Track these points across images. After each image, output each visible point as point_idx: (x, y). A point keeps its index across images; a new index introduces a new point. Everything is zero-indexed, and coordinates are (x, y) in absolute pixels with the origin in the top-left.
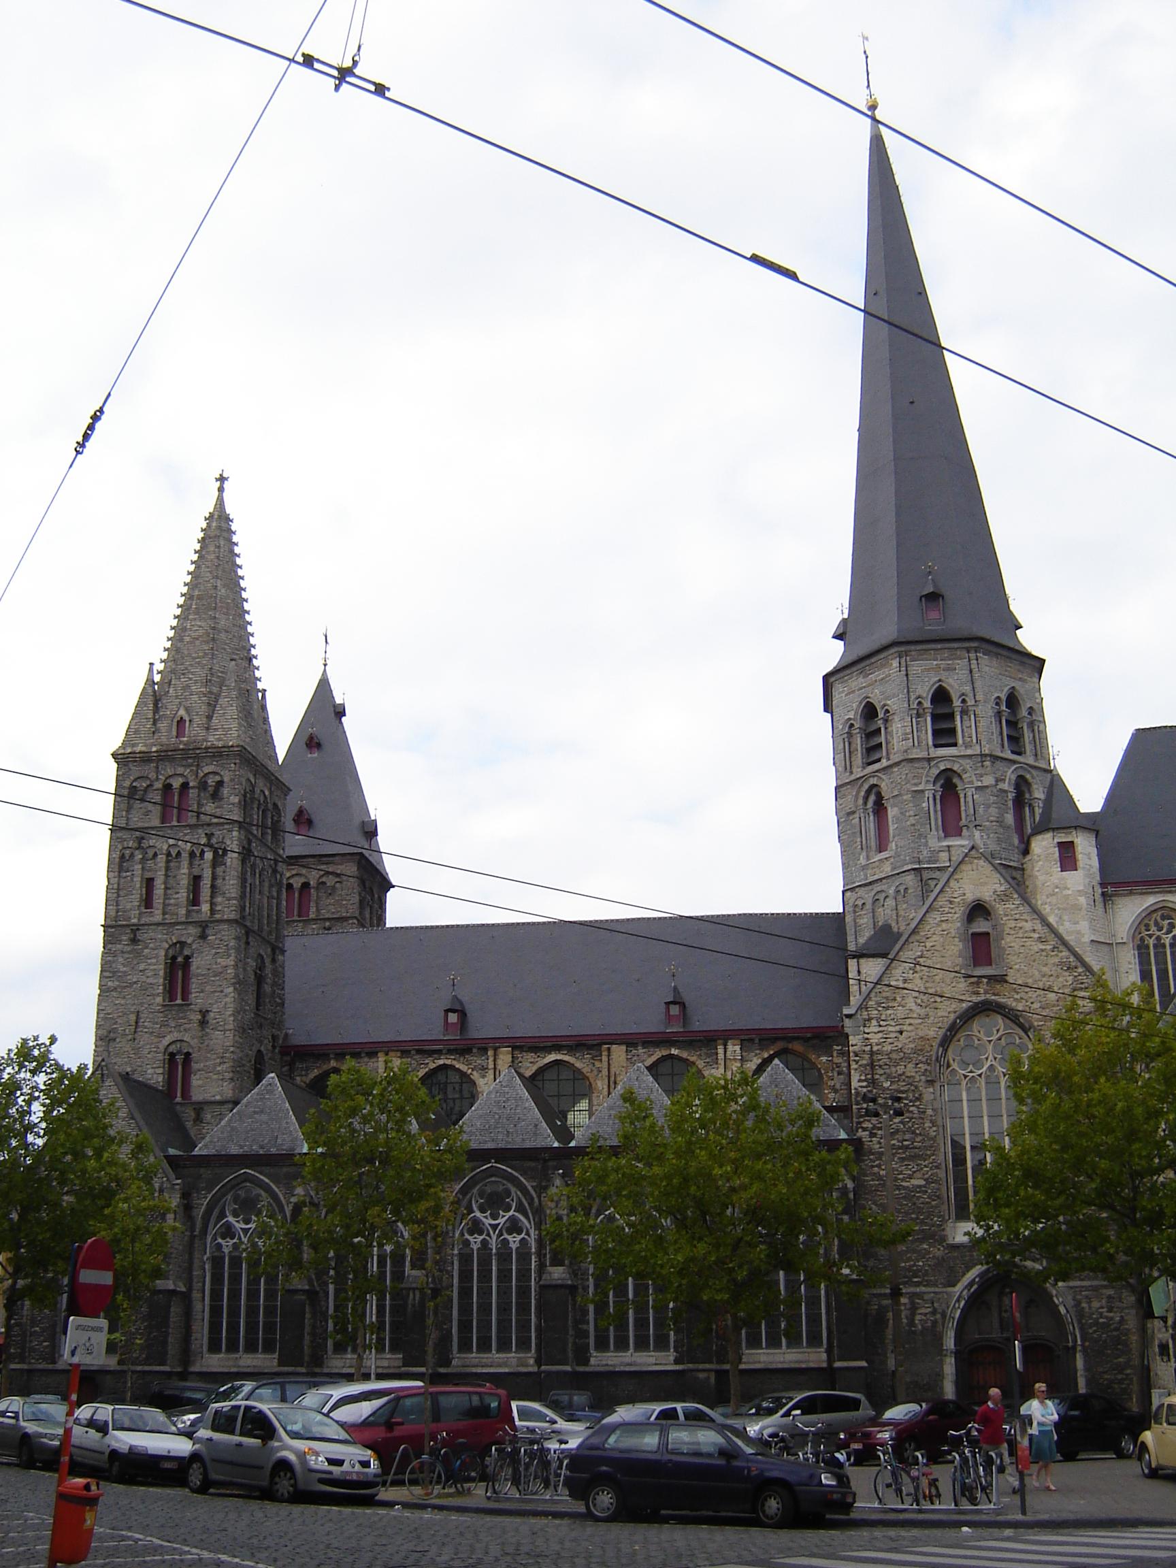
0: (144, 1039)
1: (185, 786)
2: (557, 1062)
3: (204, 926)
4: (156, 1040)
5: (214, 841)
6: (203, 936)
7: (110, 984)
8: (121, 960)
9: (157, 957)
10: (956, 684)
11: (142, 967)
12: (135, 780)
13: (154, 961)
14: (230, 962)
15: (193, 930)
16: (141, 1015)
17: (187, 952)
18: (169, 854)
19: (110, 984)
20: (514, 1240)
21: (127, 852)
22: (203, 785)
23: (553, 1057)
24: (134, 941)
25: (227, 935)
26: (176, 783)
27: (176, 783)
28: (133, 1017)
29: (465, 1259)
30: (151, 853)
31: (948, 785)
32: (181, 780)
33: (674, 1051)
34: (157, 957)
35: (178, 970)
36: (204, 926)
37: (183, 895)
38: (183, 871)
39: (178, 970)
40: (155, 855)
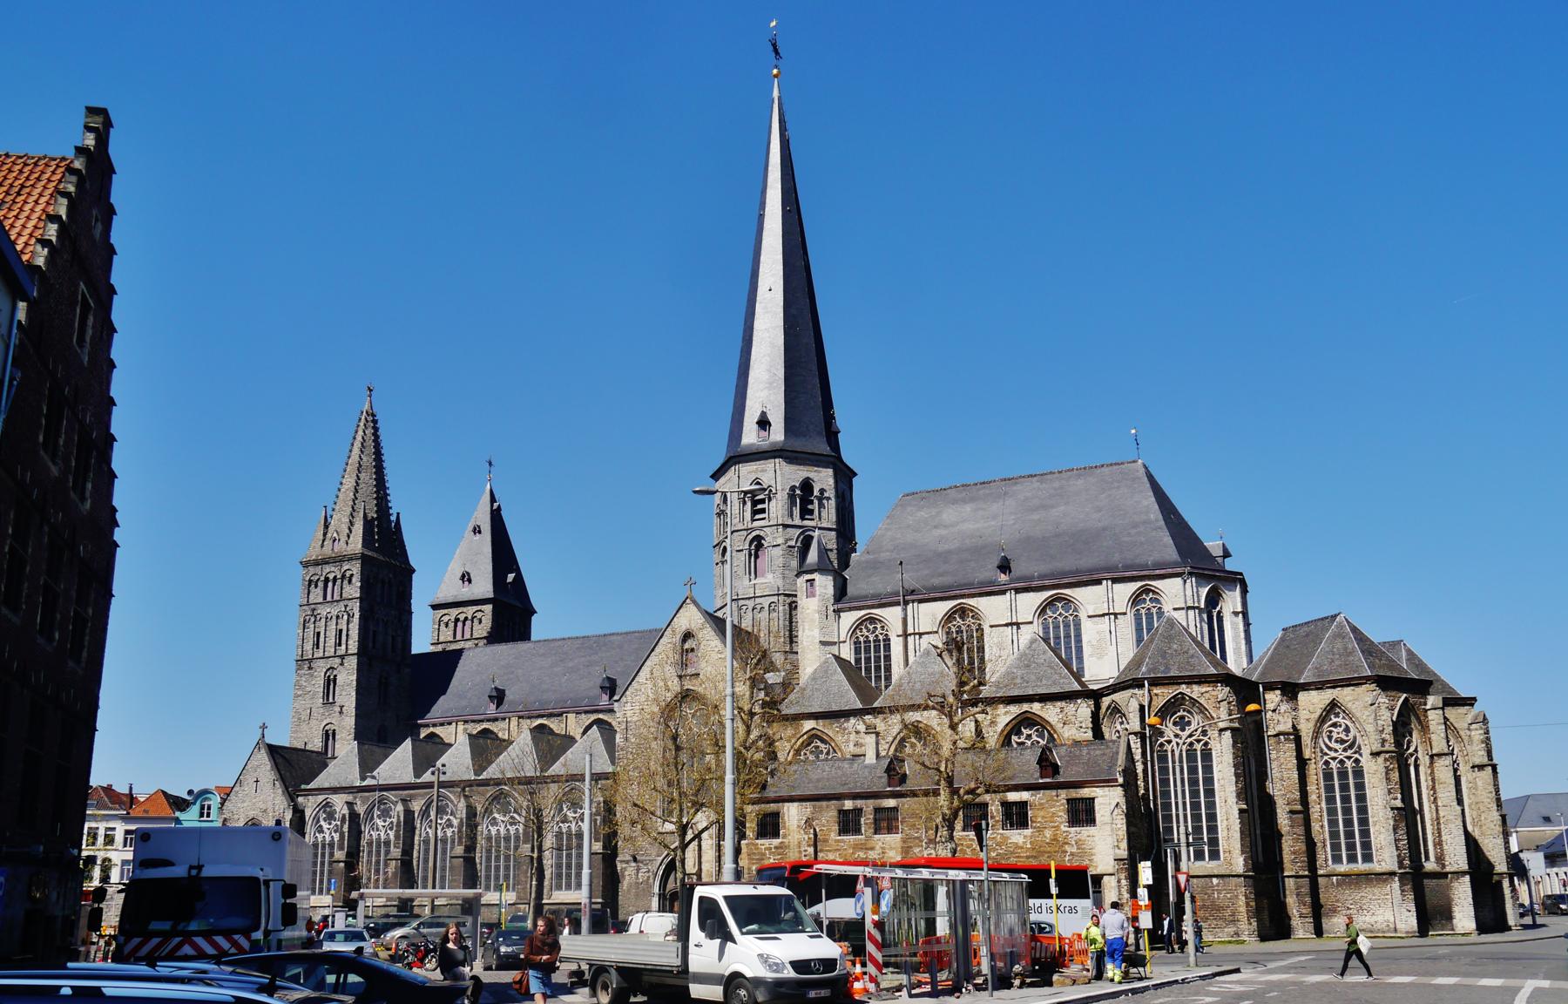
0: (313, 722)
1: (335, 579)
2: (542, 726)
3: (342, 657)
10: (767, 480)
15: (338, 660)
20: (512, 830)
22: (343, 577)
23: (540, 721)
25: (352, 662)
26: (331, 576)
27: (331, 576)
29: (427, 842)
31: (758, 542)
33: (601, 716)
35: (330, 682)
36: (342, 657)
37: (331, 641)
38: (332, 626)
39: (330, 682)
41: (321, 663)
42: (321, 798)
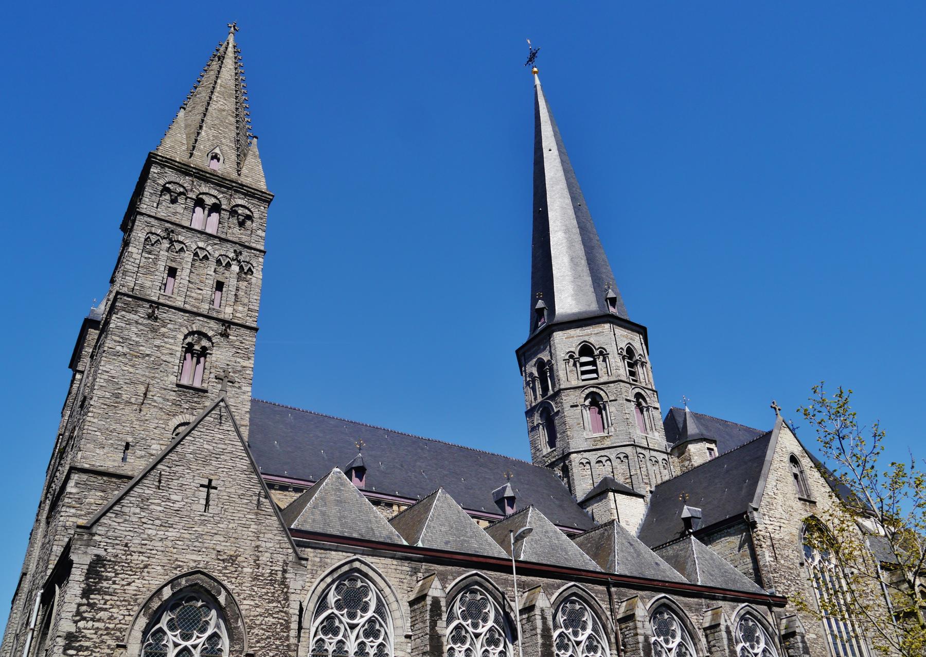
0: (149, 412)
4: (165, 417)
5: (241, 258)
6: (225, 335)
7: (119, 348)
8: (135, 330)
9: (174, 338)
11: (157, 342)
12: (169, 183)
13: (172, 341)
14: (250, 363)
16: (151, 388)
17: (205, 343)
18: (196, 254)
19: (119, 348)
21: (154, 238)
24: (150, 316)
28: (142, 389)
30: (178, 246)
32: (214, 200)
34: (174, 338)
40: (182, 250)
41: (180, 318)
42: (337, 558)
